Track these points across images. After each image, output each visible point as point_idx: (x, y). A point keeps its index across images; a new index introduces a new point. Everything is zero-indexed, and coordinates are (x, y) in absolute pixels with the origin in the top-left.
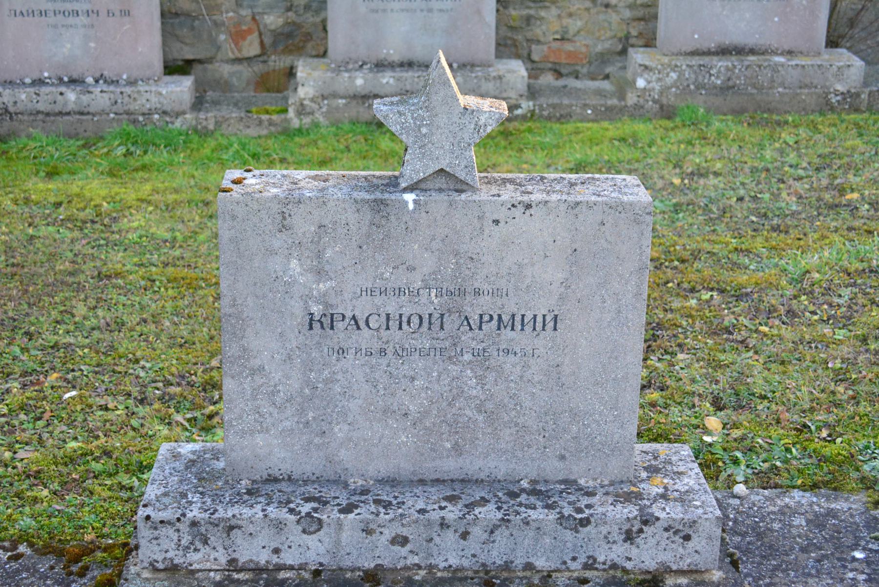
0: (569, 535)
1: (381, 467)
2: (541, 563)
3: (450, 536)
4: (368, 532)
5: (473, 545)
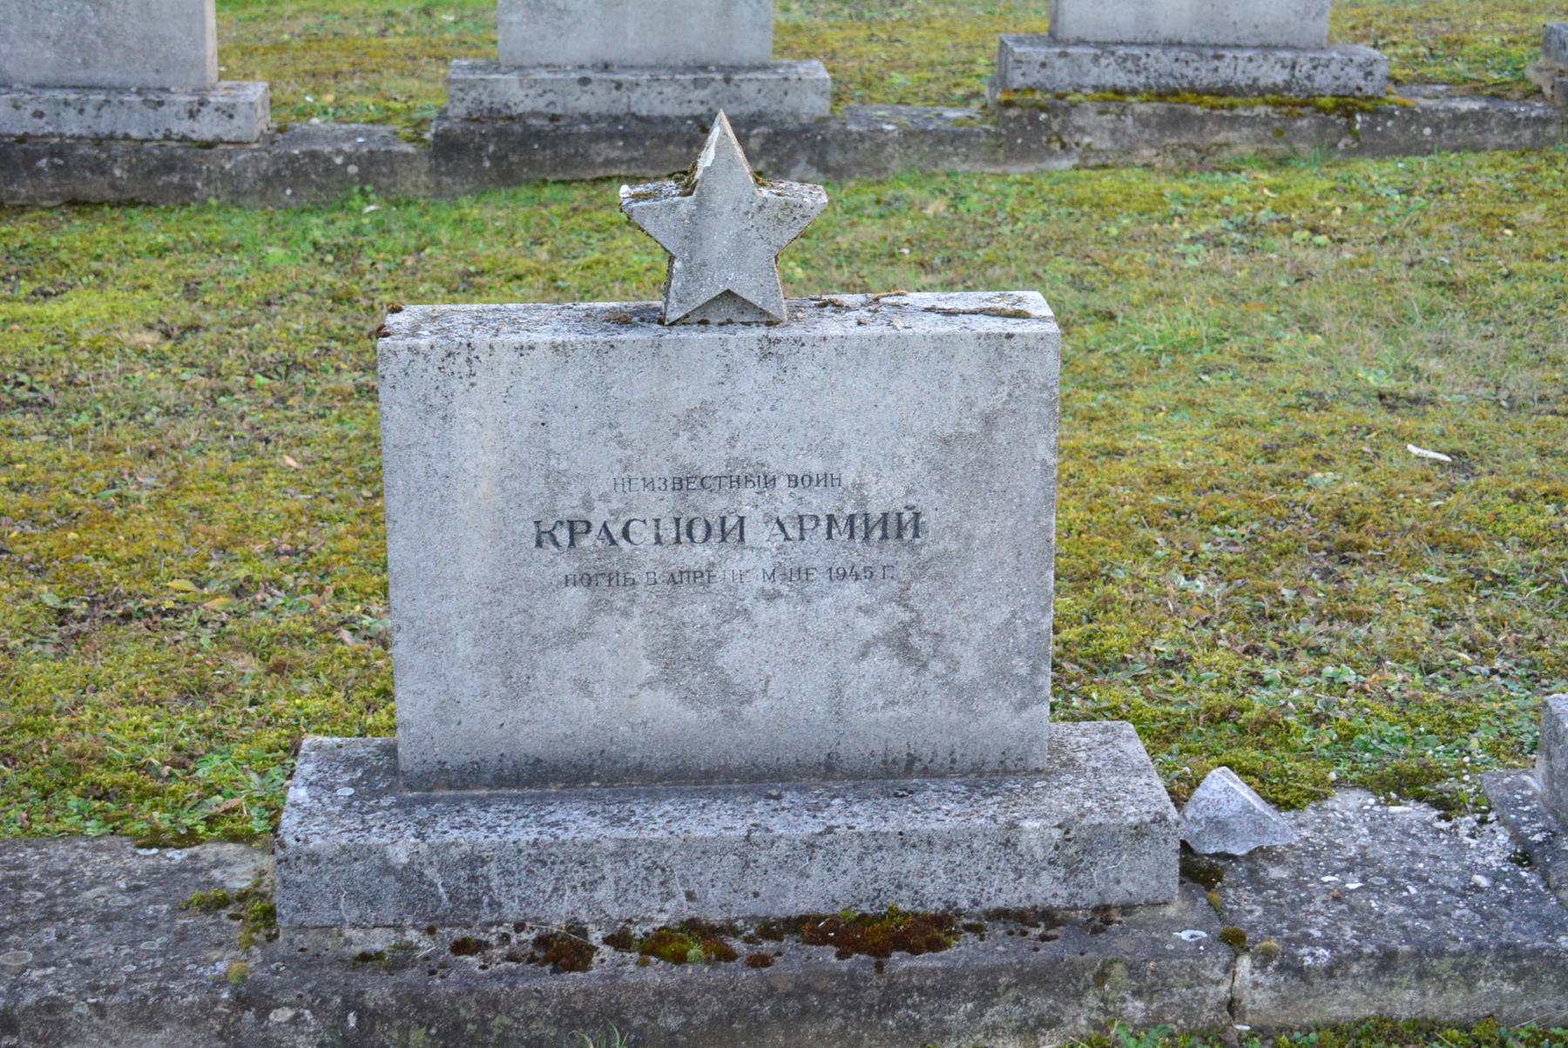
0: (151, 112)
1: (34, 76)
2: (135, 133)
3: (72, 112)
4: (17, 107)
5: (88, 118)
